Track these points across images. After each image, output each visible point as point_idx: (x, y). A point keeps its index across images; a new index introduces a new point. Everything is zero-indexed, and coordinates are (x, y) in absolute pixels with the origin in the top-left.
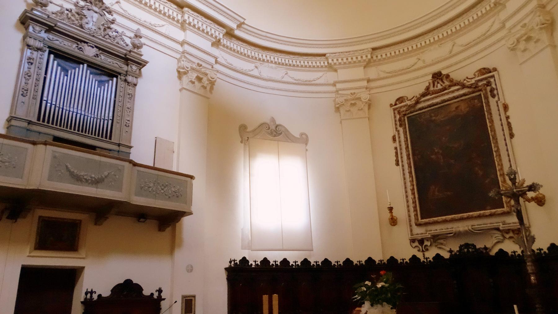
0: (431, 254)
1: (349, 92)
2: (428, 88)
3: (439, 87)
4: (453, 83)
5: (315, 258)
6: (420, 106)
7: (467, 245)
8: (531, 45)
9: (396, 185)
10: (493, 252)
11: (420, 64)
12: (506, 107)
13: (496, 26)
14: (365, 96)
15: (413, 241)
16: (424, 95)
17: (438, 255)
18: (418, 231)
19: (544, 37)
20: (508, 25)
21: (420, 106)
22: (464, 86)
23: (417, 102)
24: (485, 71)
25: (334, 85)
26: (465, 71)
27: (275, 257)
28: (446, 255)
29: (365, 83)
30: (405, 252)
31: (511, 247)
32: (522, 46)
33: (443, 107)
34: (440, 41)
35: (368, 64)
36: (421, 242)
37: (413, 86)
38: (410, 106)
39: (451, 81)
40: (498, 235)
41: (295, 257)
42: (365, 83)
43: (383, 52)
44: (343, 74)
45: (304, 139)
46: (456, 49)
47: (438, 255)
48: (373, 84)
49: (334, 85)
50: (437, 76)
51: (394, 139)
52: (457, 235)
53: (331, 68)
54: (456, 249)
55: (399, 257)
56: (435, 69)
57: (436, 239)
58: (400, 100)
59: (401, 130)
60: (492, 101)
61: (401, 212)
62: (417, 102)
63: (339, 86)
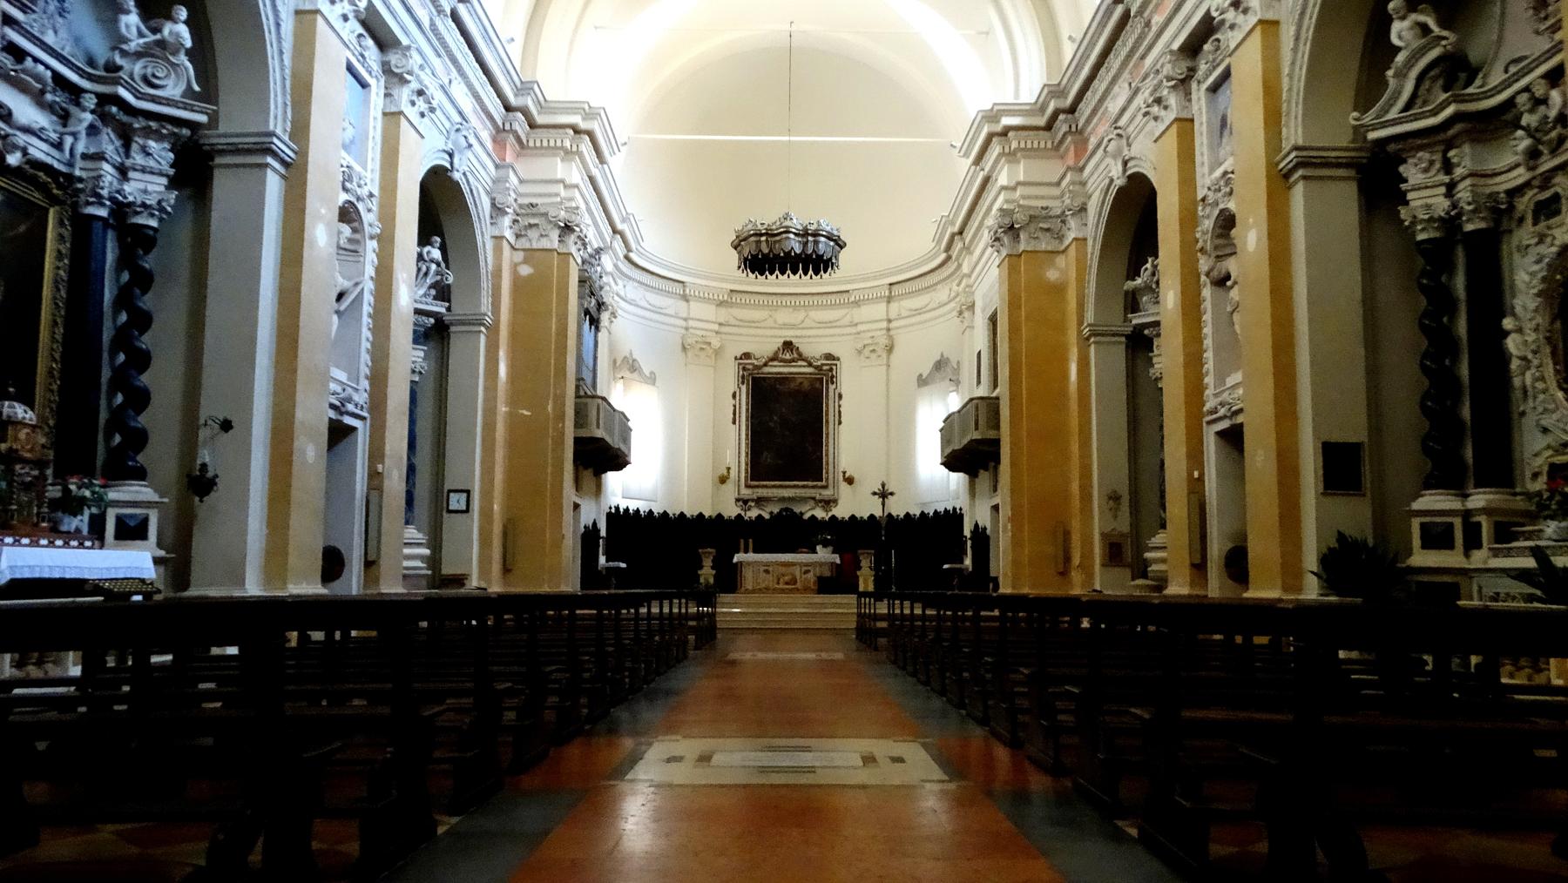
0: (753, 514)
1: (700, 333)
2: (776, 353)
3: (788, 356)
4: (801, 357)
5: (657, 510)
6: (766, 370)
7: (787, 509)
8: (874, 356)
9: (733, 448)
10: (806, 516)
11: (770, 323)
12: (840, 396)
13: (846, 321)
14: (716, 343)
15: (738, 500)
16: (772, 359)
17: (760, 516)
18: (746, 493)
19: (884, 355)
20: (860, 328)
21: (766, 370)
22: (810, 365)
23: (765, 365)
24: (829, 357)
25: (685, 320)
26: (813, 348)
27: (633, 505)
28: (767, 516)
29: (716, 327)
30: (731, 511)
31: (820, 514)
32: (866, 352)
33: (784, 379)
34: (795, 308)
35: (721, 304)
36: (745, 502)
37: (764, 345)
38: (757, 367)
39: (800, 355)
40: (812, 503)
41: (643, 507)
42: (716, 327)
43: (739, 296)
44: (699, 310)
45: (652, 380)
46: (808, 323)
47: (760, 516)
48: (724, 329)
49: (685, 320)
50: (788, 345)
51: (734, 396)
52: (783, 499)
53: (685, 298)
54: (776, 511)
55: (726, 515)
56: (789, 335)
57: (760, 501)
58: (747, 355)
59: (744, 388)
60: (832, 387)
61: (733, 473)
62: (765, 365)
63: (691, 323)
